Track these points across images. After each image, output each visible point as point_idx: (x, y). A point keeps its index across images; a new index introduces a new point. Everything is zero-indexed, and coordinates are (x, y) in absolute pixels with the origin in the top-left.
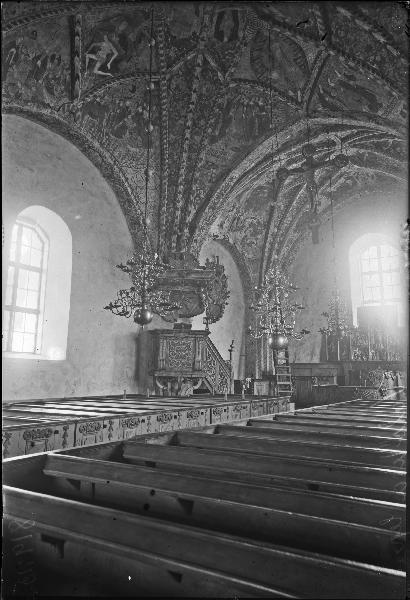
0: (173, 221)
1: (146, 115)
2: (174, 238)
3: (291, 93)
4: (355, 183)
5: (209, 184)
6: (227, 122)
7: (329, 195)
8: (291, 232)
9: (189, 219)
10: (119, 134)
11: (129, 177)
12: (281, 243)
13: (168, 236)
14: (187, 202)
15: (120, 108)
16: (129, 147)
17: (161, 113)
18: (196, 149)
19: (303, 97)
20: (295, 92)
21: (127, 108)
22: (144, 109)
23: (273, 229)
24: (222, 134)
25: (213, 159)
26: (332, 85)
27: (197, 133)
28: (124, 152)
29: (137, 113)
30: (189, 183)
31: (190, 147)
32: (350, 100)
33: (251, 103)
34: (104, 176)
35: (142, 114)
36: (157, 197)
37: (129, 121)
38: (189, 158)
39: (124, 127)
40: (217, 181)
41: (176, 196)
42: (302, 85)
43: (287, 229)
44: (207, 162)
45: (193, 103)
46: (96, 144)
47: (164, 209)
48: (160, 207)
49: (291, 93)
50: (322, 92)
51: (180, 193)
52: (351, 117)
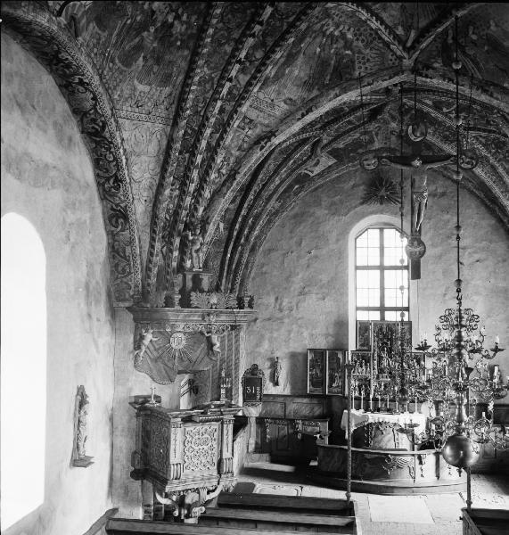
0: (176, 213)
1: (179, 28)
2: (177, 241)
3: (400, 31)
4: (371, 141)
5: (238, 153)
6: (290, 59)
7: (334, 153)
8: (272, 202)
9: (201, 210)
10: (128, 60)
11: (125, 135)
12: (257, 217)
13: (168, 240)
14: (203, 180)
15: (143, 11)
16: (136, 82)
17: (202, 30)
18: (238, 98)
19: (417, 41)
20: (408, 29)
21: (153, 12)
22: (178, 17)
23: (251, 197)
24: (278, 77)
25: (253, 114)
26: (474, 37)
27: (243, 71)
28: (127, 92)
29: (165, 23)
30: (212, 150)
31: (230, 92)
32: (491, 66)
33: (336, 33)
34: (82, 132)
35: (172, 25)
36: (158, 170)
37: (149, 36)
38: (222, 110)
39: (139, 48)
40: (251, 148)
41: (188, 169)
42: (423, 23)
43: (269, 199)
44: (245, 117)
45: (261, 23)
46: (96, 81)
47: (167, 192)
48: (161, 186)
49: (400, 31)
50: (450, 41)
51: (196, 167)
52: (485, 91)
